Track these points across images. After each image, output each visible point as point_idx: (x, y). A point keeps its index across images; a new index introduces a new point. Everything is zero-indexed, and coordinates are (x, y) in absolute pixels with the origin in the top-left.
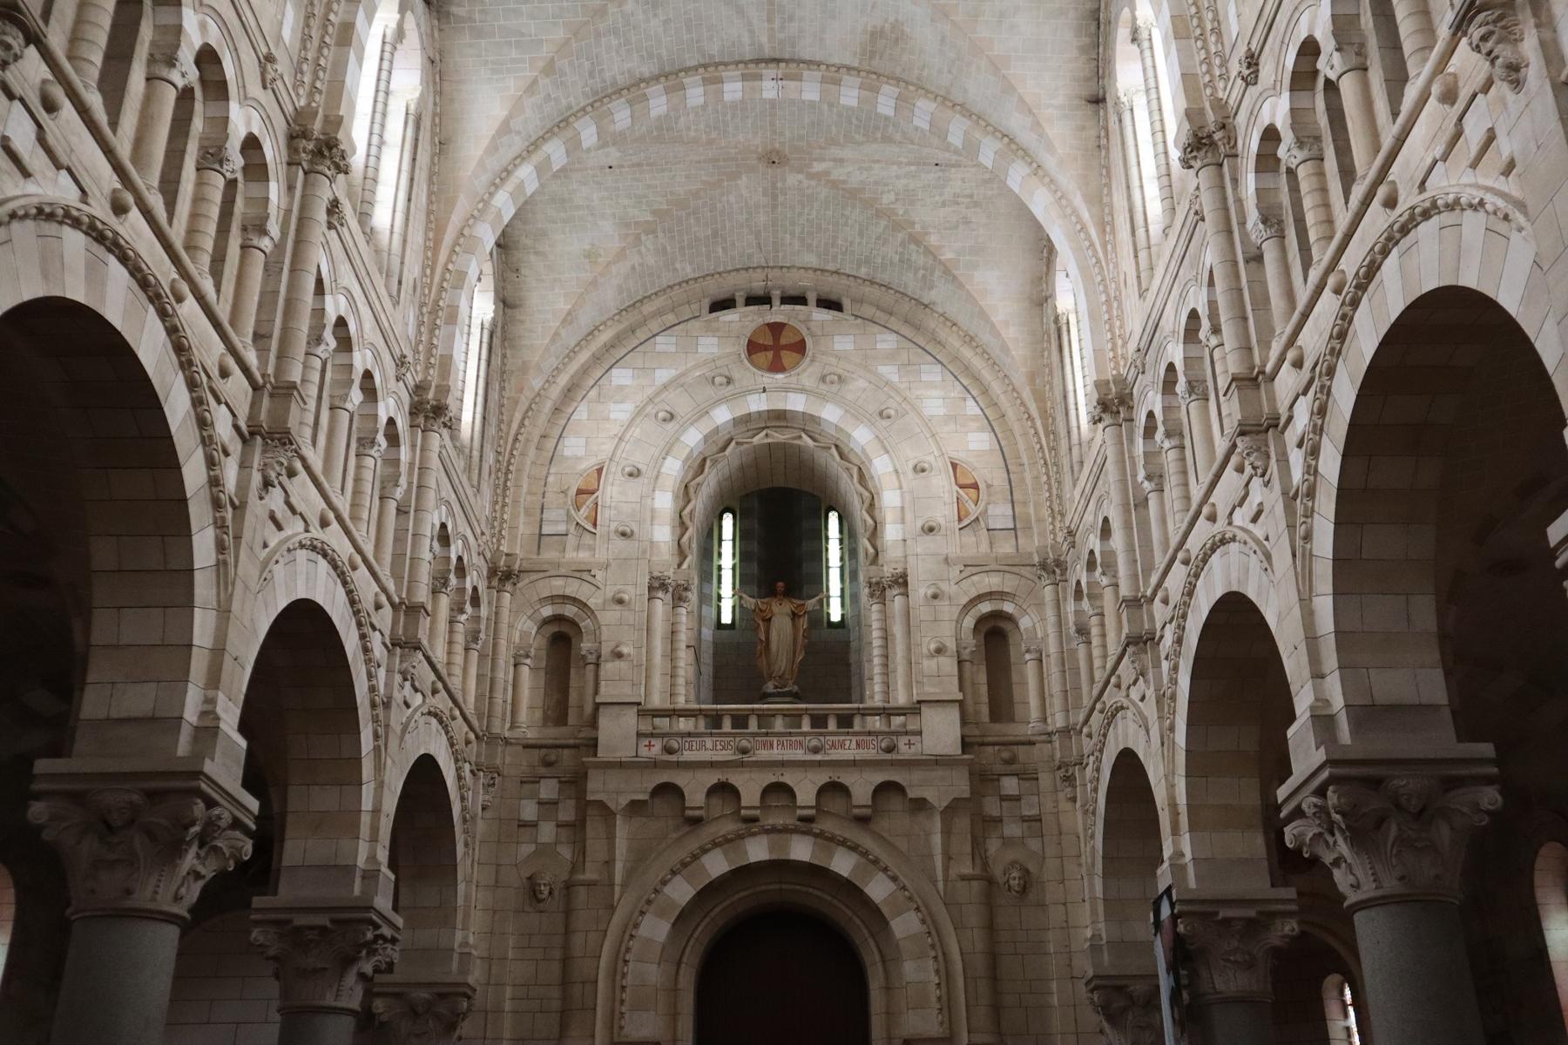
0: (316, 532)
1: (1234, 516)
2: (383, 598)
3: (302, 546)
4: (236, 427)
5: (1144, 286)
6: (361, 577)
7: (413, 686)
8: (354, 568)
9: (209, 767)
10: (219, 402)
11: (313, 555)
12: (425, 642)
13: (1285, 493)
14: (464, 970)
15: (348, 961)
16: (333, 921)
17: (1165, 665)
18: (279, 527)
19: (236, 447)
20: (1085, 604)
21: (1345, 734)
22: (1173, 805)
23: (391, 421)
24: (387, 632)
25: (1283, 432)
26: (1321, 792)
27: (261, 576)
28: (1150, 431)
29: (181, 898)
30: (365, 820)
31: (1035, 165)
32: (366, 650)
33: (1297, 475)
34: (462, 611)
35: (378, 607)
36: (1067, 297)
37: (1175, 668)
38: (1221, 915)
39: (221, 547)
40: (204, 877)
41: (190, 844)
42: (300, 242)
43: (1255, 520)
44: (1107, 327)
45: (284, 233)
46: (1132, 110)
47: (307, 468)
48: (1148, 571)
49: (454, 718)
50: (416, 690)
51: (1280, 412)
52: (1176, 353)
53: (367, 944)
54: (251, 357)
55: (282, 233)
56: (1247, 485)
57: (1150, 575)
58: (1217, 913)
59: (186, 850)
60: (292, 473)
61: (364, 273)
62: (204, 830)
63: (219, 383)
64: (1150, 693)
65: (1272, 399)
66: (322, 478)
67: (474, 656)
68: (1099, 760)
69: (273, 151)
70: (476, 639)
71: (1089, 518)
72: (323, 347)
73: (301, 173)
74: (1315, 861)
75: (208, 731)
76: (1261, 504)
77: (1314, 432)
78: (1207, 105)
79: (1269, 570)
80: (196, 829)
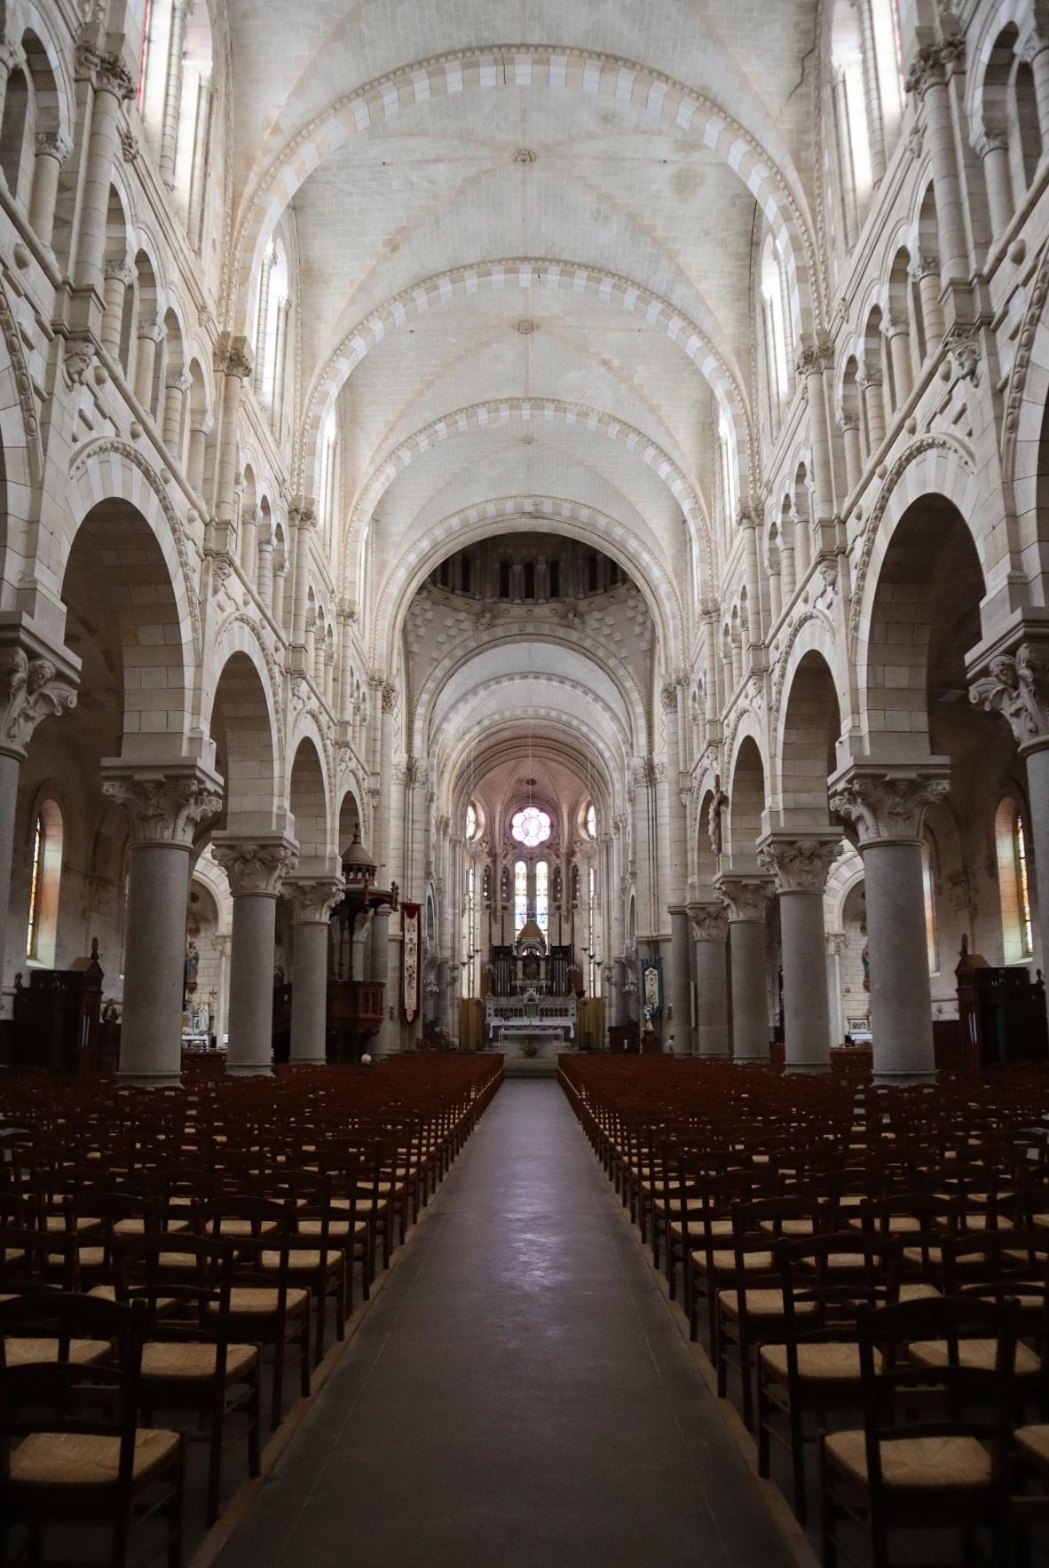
0: (126, 438)
1: (933, 425)
2: (195, 513)
3: (116, 450)
4: (39, 323)
5: (850, 245)
7: (226, 594)
8: (166, 481)
9: (26, 620)
10: (19, 295)
11: (128, 462)
12: (238, 562)
13: (993, 387)
14: (282, 828)
15: (178, 808)
16: (166, 777)
17: (854, 574)
18: (90, 428)
19: (42, 343)
20: (779, 540)
21: (1039, 600)
22: (854, 691)
23: (195, 363)
24: (201, 544)
25: (995, 331)
26: (1011, 651)
27: (71, 467)
28: (849, 377)
29: (14, 736)
30: (188, 695)
31: (754, 143)
32: (181, 553)
33: (1007, 367)
34: (269, 542)
35: (191, 520)
36: (772, 283)
37: (863, 577)
38: (888, 778)
39: (29, 430)
40: (34, 718)
41: (18, 689)
42: (93, 156)
43: (955, 422)
44: (814, 288)
45: (78, 144)
46: (844, 81)
47: (115, 380)
48: (841, 497)
50: (229, 598)
51: (995, 310)
52: (881, 295)
53: (192, 794)
54: (51, 257)
55: (75, 145)
56: (950, 391)
57: (843, 502)
58: (885, 776)
59: (14, 696)
60: (100, 381)
61: (163, 216)
62: (30, 677)
63: (14, 271)
64: (838, 600)
65: (987, 299)
66: (134, 400)
68: (784, 669)
69: (59, 59)
70: (282, 567)
71: (785, 470)
72: (125, 272)
73: (90, 88)
74: (996, 715)
75: (27, 594)
76: (965, 405)
77: (1031, 323)
78: (937, 23)
79: (970, 463)
80: (21, 675)
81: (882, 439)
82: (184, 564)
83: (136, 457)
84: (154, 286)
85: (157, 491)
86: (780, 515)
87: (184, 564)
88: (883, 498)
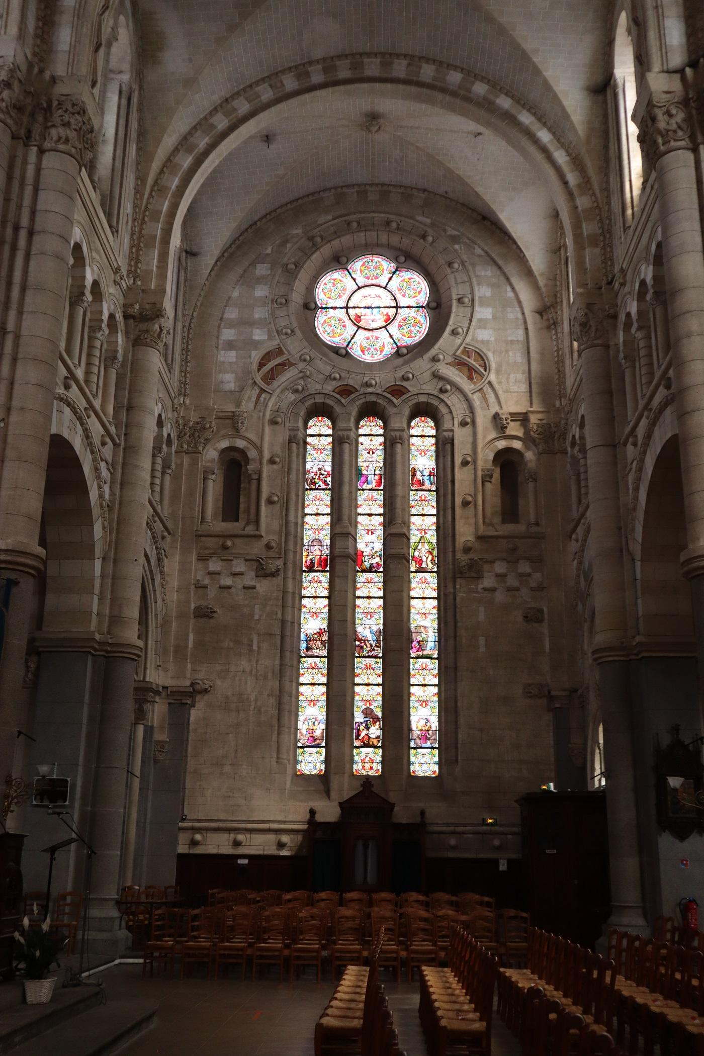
6: (93, 424)
32: (97, 469)
35: (104, 444)
49: (155, 522)
67: (167, 478)
81: (651, 382)
82: (98, 477)
83: (67, 400)
84: (84, 266)
85: (82, 424)
86: (578, 429)
87: (98, 477)
88: (649, 429)
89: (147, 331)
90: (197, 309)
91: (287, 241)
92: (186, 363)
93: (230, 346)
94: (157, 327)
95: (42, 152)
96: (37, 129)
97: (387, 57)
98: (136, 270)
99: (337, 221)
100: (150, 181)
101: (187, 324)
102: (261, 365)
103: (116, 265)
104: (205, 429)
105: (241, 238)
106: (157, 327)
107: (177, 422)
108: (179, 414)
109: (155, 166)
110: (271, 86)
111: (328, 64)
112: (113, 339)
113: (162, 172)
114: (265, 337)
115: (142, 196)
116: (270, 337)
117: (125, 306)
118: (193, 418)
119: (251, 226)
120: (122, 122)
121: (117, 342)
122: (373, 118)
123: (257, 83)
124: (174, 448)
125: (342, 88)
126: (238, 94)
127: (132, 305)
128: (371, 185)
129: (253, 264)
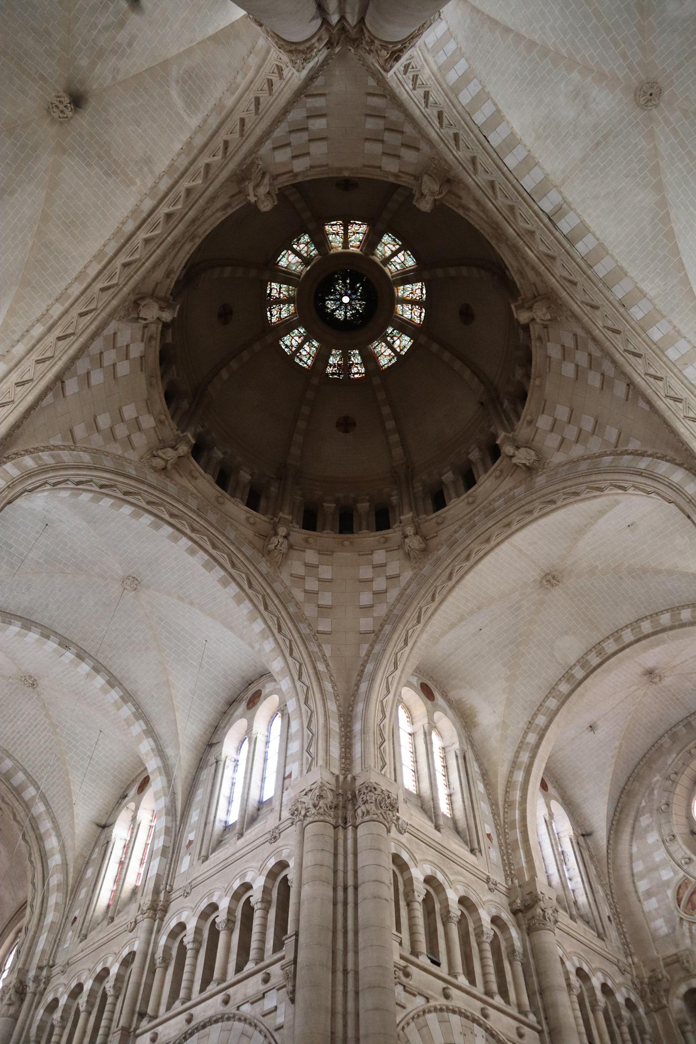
89: (533, 918)
90: (612, 876)
91: (653, 789)
92: (621, 925)
93: (649, 894)
94: (539, 911)
95: (356, 827)
96: (349, 814)
97: (616, 635)
98: (511, 873)
99: (679, 756)
100: (501, 802)
101: (608, 892)
102: (679, 901)
103: (485, 877)
104: (659, 980)
105: (619, 805)
106: (539, 911)
107: (633, 983)
108: (632, 975)
109: (500, 791)
110: (554, 697)
111: (582, 662)
112: (508, 936)
113: (507, 792)
114: (672, 874)
115: (499, 816)
116: (675, 872)
117: (510, 904)
118: (646, 974)
119: (622, 792)
120: (463, 774)
121: (511, 937)
122: (650, 673)
123: (544, 701)
124: (641, 1011)
125: (599, 670)
126: (536, 714)
127: (514, 901)
128: (690, 716)
129: (636, 820)
